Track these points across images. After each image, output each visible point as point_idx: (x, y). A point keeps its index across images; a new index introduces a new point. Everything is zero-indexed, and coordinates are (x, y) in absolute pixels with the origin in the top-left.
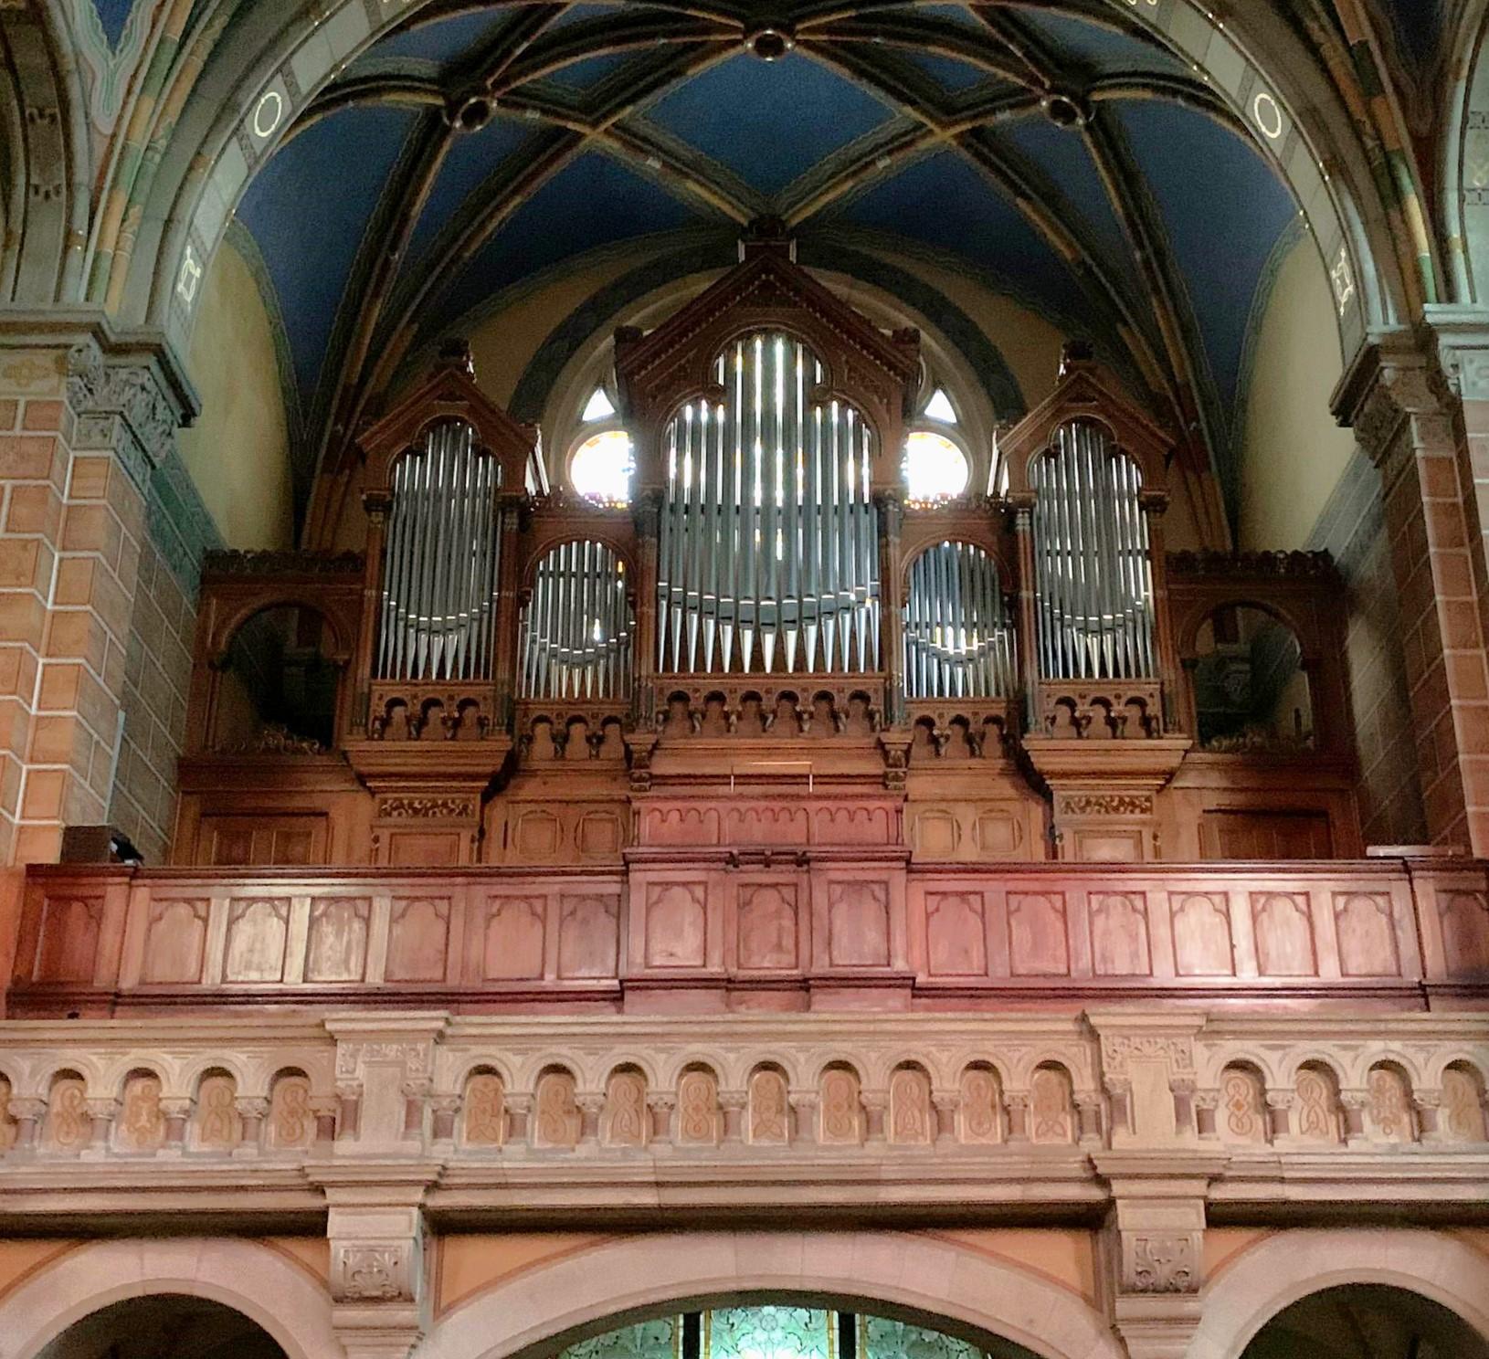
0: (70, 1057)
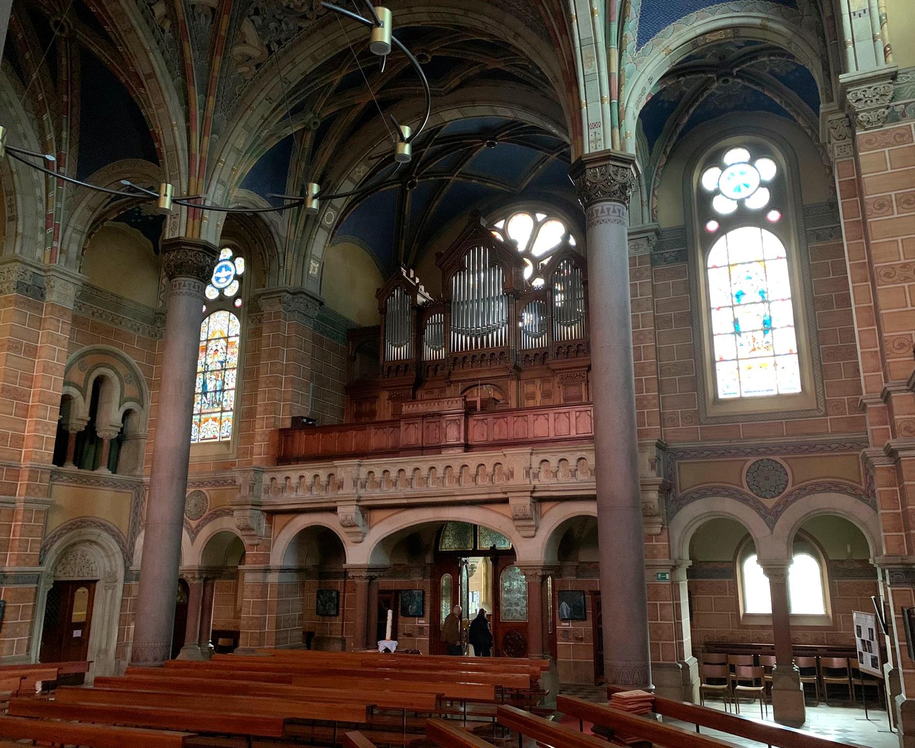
0: (287, 474)
